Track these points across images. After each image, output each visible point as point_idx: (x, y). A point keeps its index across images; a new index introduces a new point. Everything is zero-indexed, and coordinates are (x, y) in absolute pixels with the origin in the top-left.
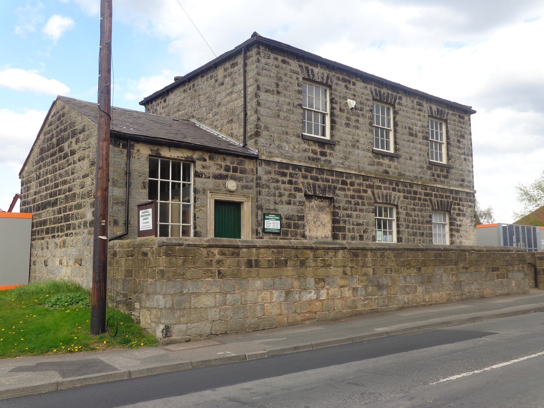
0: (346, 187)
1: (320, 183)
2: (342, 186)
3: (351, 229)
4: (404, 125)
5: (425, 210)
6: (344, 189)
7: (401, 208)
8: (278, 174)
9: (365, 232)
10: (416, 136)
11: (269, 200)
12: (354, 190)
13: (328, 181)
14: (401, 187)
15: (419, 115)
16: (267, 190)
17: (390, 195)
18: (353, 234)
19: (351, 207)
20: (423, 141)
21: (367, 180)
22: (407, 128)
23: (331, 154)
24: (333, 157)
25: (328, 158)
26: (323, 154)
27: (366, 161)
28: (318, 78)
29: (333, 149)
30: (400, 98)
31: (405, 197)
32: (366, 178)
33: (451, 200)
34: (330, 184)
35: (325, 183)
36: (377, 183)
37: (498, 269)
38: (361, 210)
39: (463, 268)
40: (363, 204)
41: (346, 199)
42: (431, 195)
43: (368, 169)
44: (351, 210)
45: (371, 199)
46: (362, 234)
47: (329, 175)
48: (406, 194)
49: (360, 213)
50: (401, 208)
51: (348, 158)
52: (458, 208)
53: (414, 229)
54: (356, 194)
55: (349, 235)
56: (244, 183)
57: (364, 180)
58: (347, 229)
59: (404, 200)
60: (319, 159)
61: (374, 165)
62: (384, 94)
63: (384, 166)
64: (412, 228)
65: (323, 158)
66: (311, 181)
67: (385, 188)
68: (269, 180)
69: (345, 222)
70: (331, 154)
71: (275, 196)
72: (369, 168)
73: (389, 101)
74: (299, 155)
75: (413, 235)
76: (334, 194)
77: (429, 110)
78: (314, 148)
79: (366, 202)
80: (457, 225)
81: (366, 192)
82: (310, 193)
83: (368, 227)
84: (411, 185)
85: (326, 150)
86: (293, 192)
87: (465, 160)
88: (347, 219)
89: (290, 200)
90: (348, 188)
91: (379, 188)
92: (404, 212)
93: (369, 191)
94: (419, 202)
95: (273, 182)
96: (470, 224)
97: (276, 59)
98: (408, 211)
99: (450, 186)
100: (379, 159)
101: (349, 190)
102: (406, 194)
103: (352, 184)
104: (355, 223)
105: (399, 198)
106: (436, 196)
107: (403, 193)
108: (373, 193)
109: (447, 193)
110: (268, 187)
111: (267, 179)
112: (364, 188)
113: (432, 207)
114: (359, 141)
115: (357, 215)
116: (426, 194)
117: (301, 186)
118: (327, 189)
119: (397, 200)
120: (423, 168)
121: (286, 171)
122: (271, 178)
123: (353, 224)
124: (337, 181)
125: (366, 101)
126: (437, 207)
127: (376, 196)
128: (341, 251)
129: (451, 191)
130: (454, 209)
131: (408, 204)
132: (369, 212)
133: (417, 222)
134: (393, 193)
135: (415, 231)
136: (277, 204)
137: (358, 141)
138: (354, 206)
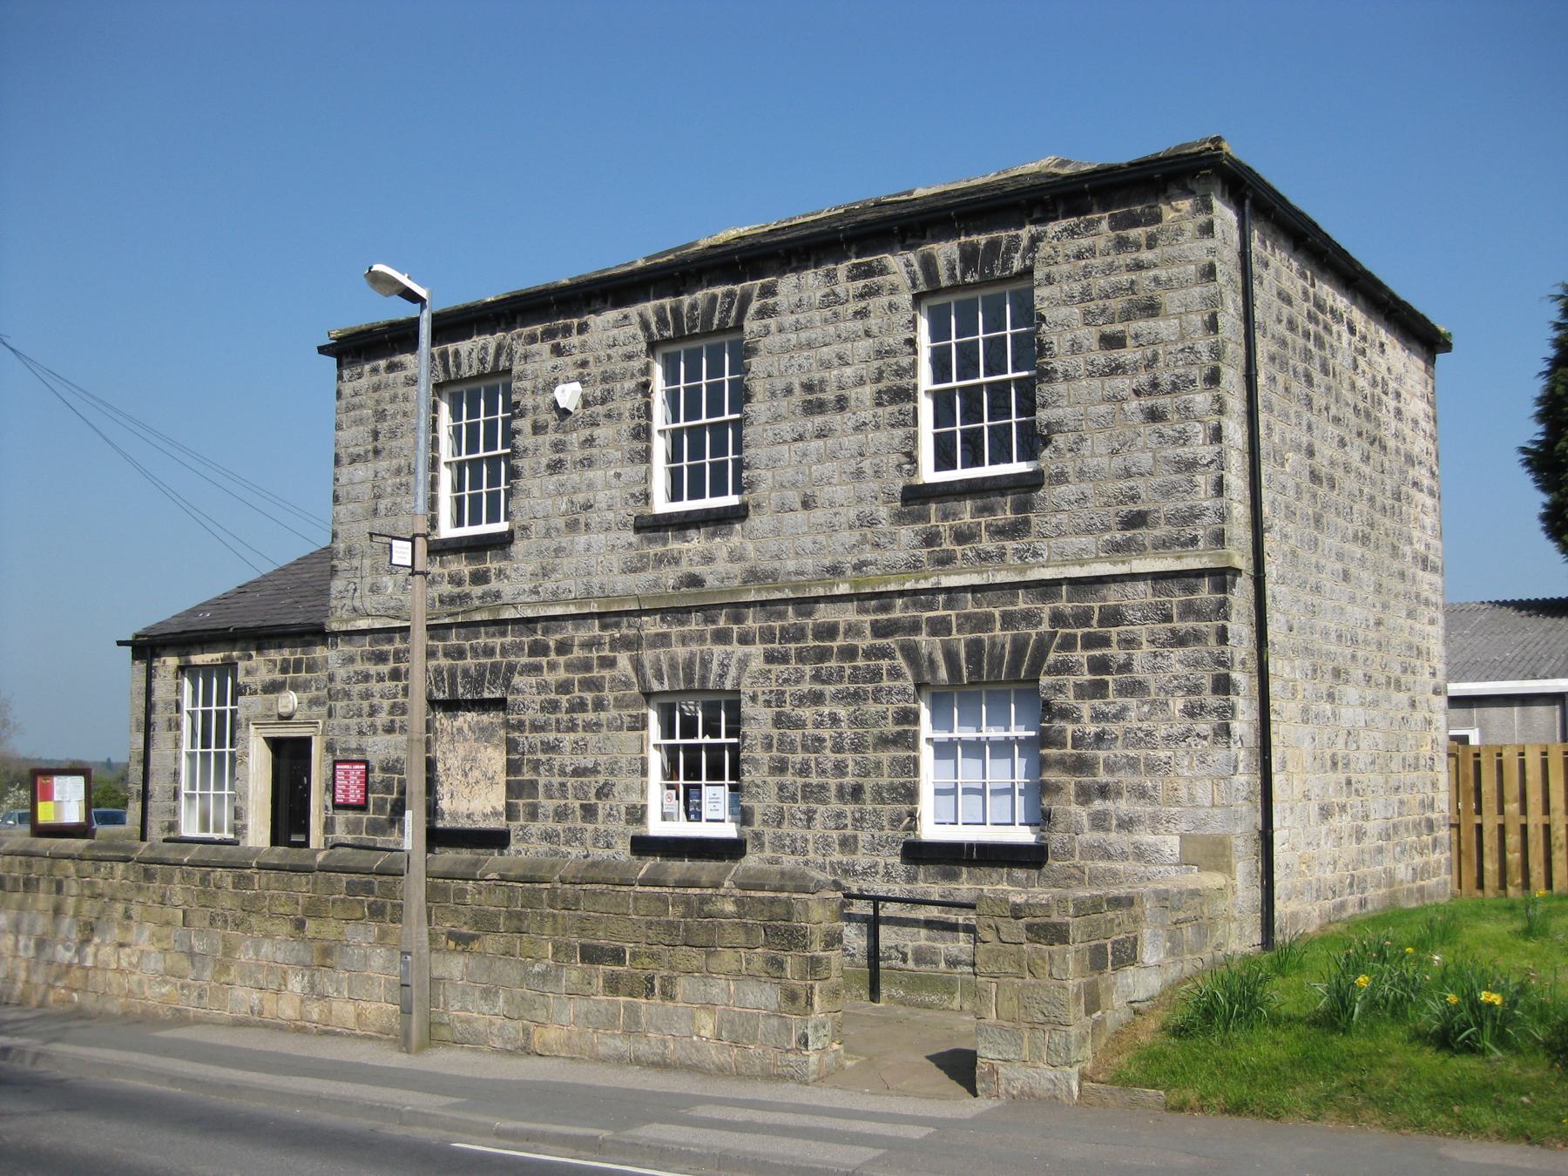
0: (544, 661)
1: (470, 662)
2: (532, 660)
3: (556, 785)
4: (780, 384)
6: (537, 669)
7: (754, 698)
8: (369, 659)
9: (602, 792)
10: (841, 404)
11: (348, 728)
12: (569, 667)
13: (489, 652)
14: (752, 623)
15: (862, 314)
16: (345, 702)
17: (702, 660)
18: (563, 802)
19: (558, 721)
20: (880, 411)
21: (617, 625)
22: (797, 389)
23: (500, 572)
24: (508, 578)
25: (494, 585)
26: (480, 578)
27: (615, 561)
28: (471, 367)
29: (507, 557)
30: (768, 291)
31: (770, 658)
33: (1045, 627)
34: (498, 658)
35: (483, 661)
36: (652, 626)
37: (617, 956)
38: (590, 727)
39: (451, 935)
40: (599, 705)
41: (543, 697)
42: (915, 627)
43: (619, 587)
44: (559, 730)
45: (627, 684)
46: (593, 801)
47: (494, 635)
48: (776, 646)
49: (589, 736)
50: (754, 698)
51: (554, 570)
53: (814, 775)
54: (577, 677)
55: (547, 805)
56: (313, 693)
57: (603, 627)
58: (541, 789)
59: (767, 667)
60: (467, 596)
61: (643, 569)
62: (693, 307)
63: (684, 561)
64: (804, 770)
65: (478, 590)
66: (444, 662)
67: (684, 640)
68: (349, 678)
69: (536, 766)
70: (500, 573)
71: (360, 715)
73: (716, 322)
75: (804, 797)
77: (920, 275)
78: (454, 567)
79: (609, 695)
80: (1078, 741)
81: (610, 663)
82: (441, 696)
83: (612, 779)
84: (805, 604)
85: (488, 565)
87: (1154, 415)
88: (543, 757)
89: (392, 721)
90: (548, 663)
91: (662, 640)
92: (767, 714)
93: (623, 660)
95: (358, 682)
96: (1178, 729)
97: (375, 370)
98: (787, 709)
99: (1022, 571)
100: (665, 542)
101: (553, 666)
102: (776, 646)
103: (563, 648)
104: (569, 769)
105: (743, 663)
106: (939, 627)
107: (763, 640)
108: (638, 666)
109: (1012, 604)
110: (347, 695)
111: (345, 676)
112: (606, 653)
113: (917, 674)
114: (591, 506)
115: (577, 743)
116: (880, 630)
118: (488, 676)
119: (733, 672)
120: (872, 522)
121: (386, 647)
122: (355, 672)
123: (563, 773)
124: (518, 648)
125: (625, 364)
126: (943, 674)
127: (649, 672)
129: (1046, 588)
130: (1064, 668)
131: (786, 681)
132: (620, 728)
133: (829, 744)
134: (718, 650)
135: (814, 779)
136: (365, 734)
137: (588, 507)
138: (566, 717)
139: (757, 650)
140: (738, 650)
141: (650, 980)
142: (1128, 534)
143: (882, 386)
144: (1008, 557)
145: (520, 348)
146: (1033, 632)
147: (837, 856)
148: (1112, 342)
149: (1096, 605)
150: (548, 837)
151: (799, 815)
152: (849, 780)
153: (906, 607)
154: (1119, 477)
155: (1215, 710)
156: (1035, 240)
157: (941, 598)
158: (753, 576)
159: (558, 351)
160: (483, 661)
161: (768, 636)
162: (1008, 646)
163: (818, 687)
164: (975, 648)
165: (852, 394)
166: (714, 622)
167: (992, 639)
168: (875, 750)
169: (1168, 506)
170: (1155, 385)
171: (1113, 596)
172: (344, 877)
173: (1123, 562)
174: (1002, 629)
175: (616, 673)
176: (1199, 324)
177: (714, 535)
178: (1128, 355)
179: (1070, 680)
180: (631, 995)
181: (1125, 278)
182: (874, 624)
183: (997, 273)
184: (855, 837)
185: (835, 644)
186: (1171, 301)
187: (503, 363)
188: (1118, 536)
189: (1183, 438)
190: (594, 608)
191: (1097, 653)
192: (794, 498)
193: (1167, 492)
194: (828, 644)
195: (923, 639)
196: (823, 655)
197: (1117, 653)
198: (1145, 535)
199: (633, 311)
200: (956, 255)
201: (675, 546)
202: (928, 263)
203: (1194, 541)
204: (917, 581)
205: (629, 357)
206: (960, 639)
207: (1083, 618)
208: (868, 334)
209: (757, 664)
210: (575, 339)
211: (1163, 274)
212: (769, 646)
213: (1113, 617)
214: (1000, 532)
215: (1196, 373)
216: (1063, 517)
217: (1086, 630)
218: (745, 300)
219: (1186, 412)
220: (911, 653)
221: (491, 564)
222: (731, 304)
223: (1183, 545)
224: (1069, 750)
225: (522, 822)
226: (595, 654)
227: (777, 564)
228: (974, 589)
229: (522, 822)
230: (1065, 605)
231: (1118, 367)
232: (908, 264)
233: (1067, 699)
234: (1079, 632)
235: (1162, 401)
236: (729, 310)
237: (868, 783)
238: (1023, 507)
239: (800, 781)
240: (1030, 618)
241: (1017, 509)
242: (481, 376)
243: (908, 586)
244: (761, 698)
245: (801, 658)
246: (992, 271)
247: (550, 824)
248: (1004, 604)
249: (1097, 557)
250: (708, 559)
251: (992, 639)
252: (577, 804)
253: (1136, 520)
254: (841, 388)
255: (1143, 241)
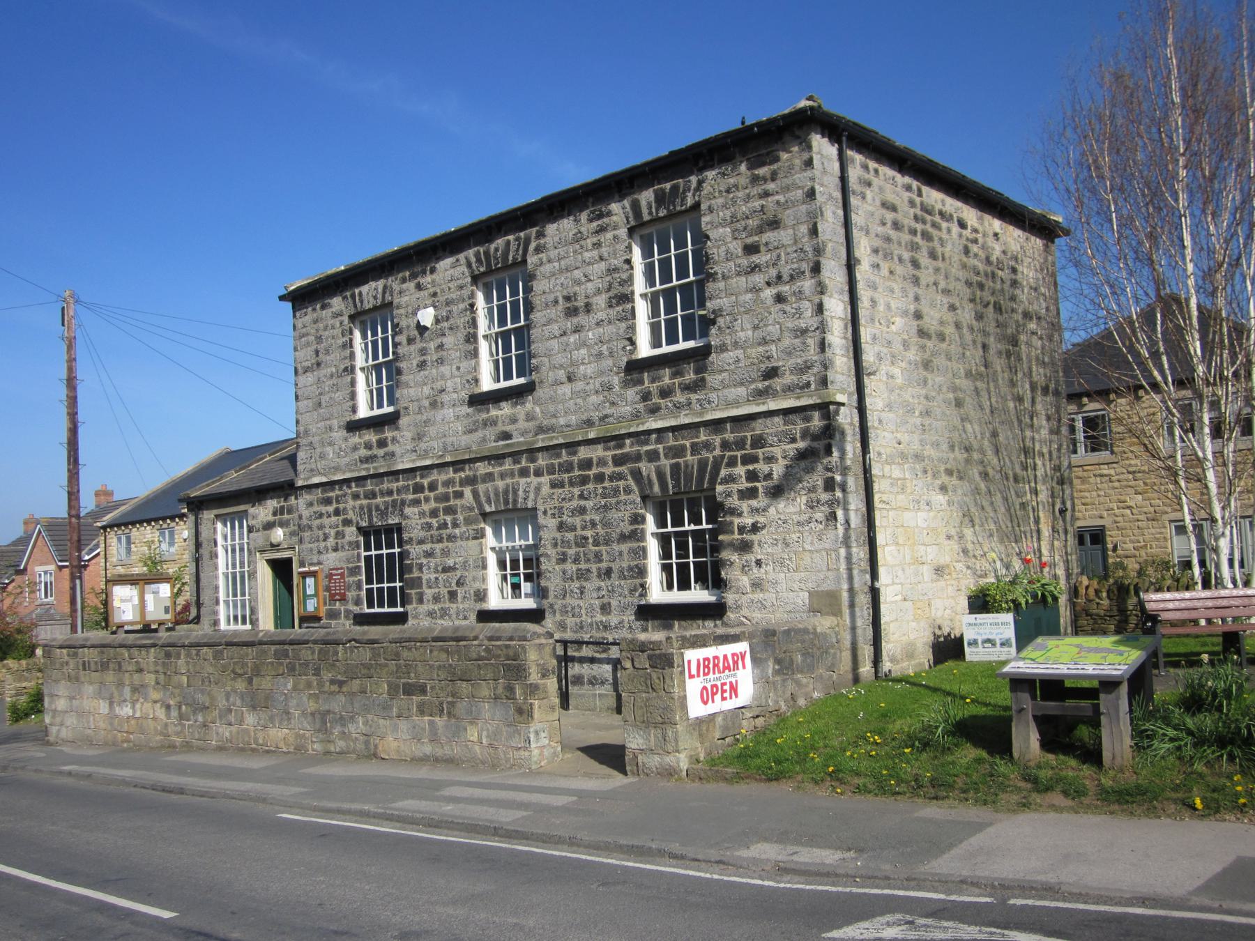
0: (422, 496)
1: (379, 500)
3: (433, 580)
4: (551, 298)
5: (618, 503)
6: (416, 502)
7: (545, 513)
9: (459, 583)
10: (588, 308)
11: (311, 550)
12: (437, 499)
13: (390, 493)
14: (542, 461)
15: (597, 245)
17: (513, 488)
19: (432, 536)
21: (463, 470)
22: (561, 300)
25: (390, 448)
26: (382, 443)
27: (459, 427)
29: (397, 429)
30: (541, 235)
31: (553, 485)
32: (458, 465)
33: (717, 452)
34: (395, 496)
35: (387, 499)
36: (482, 468)
37: (423, 690)
38: (451, 538)
39: (332, 682)
40: (455, 525)
42: (638, 458)
43: (463, 443)
44: (433, 543)
45: (471, 509)
46: (455, 588)
49: (450, 545)
50: (545, 513)
51: (425, 435)
52: (748, 472)
55: (429, 593)
56: (292, 528)
57: (455, 471)
58: (424, 582)
59: (552, 491)
60: (375, 456)
61: (476, 430)
62: (497, 250)
63: (500, 423)
64: (576, 560)
65: (381, 452)
67: (503, 476)
71: (318, 541)
72: (465, 440)
73: (511, 258)
74: (347, 459)
75: (578, 578)
76: (401, 515)
77: (631, 215)
78: (367, 437)
79: (460, 517)
80: (742, 529)
81: (459, 495)
84: (572, 446)
86: (341, 528)
87: (780, 299)
88: (424, 561)
89: (337, 543)
91: (489, 477)
92: (552, 523)
94: (598, 486)
95: (317, 518)
96: (805, 517)
97: (314, 310)
98: (565, 517)
99: (701, 414)
100: (488, 411)
101: (427, 499)
102: (556, 476)
104: (440, 568)
105: (538, 489)
106: (653, 456)
107: (549, 473)
108: (475, 494)
109: (697, 437)
112: (458, 488)
113: (641, 490)
116: (618, 461)
117: (351, 515)
119: (532, 496)
123: (436, 571)
126: (656, 488)
127: (483, 499)
128: (153, 650)
129: (717, 425)
130: (730, 479)
131: (564, 499)
132: (468, 539)
133: (591, 540)
134: (523, 481)
135: (583, 566)
139: (545, 479)
140: (534, 480)
141: (441, 704)
142: (766, 383)
143: (611, 294)
144: (693, 406)
145: (396, 286)
146: (711, 456)
147: (599, 617)
148: (751, 249)
149: (748, 434)
150: (431, 614)
151: (576, 590)
152: (604, 565)
153: (632, 445)
154: (759, 344)
155: (826, 502)
156: (700, 183)
157: (654, 436)
158: (541, 430)
159: (419, 287)
160: (387, 499)
161: (551, 470)
162: (695, 467)
163: (583, 503)
164: (675, 468)
165: (595, 300)
166: (519, 463)
167: (686, 462)
168: (618, 543)
169: (791, 362)
170: (779, 277)
171: (759, 427)
172: (273, 648)
173: (764, 403)
174: (692, 455)
175: (463, 502)
176: (806, 231)
177: (516, 404)
178: (761, 258)
179: (734, 487)
180: (431, 715)
181: (757, 204)
182: (614, 457)
183: (678, 208)
184: (609, 604)
185: (591, 473)
186: (788, 216)
187: (388, 298)
188: (760, 385)
189: (799, 313)
190: (448, 459)
191: (751, 467)
192: (561, 374)
193: (789, 353)
194: (587, 473)
195: (646, 468)
196: (584, 480)
197: (762, 467)
198: (777, 383)
199: (461, 256)
200: (652, 198)
201: (494, 412)
202: (636, 206)
203: (808, 385)
204: (638, 425)
205: (461, 287)
206: (666, 463)
207: (740, 444)
208: (601, 258)
209: (546, 490)
210: (428, 278)
211: (781, 198)
212: (552, 477)
213: (759, 442)
214: (687, 388)
215: (805, 266)
216: (725, 374)
217: (743, 452)
218: (527, 242)
219: (799, 294)
220: (637, 475)
221: (389, 434)
222: (519, 245)
223: (802, 388)
224: (736, 536)
225: (415, 605)
226: (451, 490)
227: (554, 421)
228: (673, 429)
229: (415, 605)
230: (729, 436)
231: (756, 266)
232: (624, 208)
233: (733, 502)
234: (739, 454)
235: (785, 289)
236: (517, 250)
237: (615, 566)
238: (701, 370)
239: (574, 567)
240: (708, 446)
241: (696, 372)
242: (375, 308)
243: (632, 430)
244: (549, 512)
245: (571, 484)
246: (675, 208)
247: (431, 607)
248: (692, 438)
249: (748, 400)
250: (514, 420)
251: (686, 462)
252: (446, 590)
253: (772, 373)
254: (587, 297)
255: (768, 176)
